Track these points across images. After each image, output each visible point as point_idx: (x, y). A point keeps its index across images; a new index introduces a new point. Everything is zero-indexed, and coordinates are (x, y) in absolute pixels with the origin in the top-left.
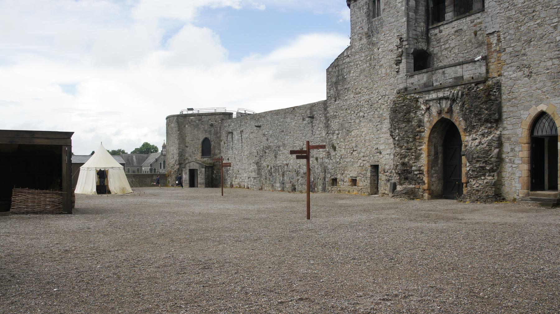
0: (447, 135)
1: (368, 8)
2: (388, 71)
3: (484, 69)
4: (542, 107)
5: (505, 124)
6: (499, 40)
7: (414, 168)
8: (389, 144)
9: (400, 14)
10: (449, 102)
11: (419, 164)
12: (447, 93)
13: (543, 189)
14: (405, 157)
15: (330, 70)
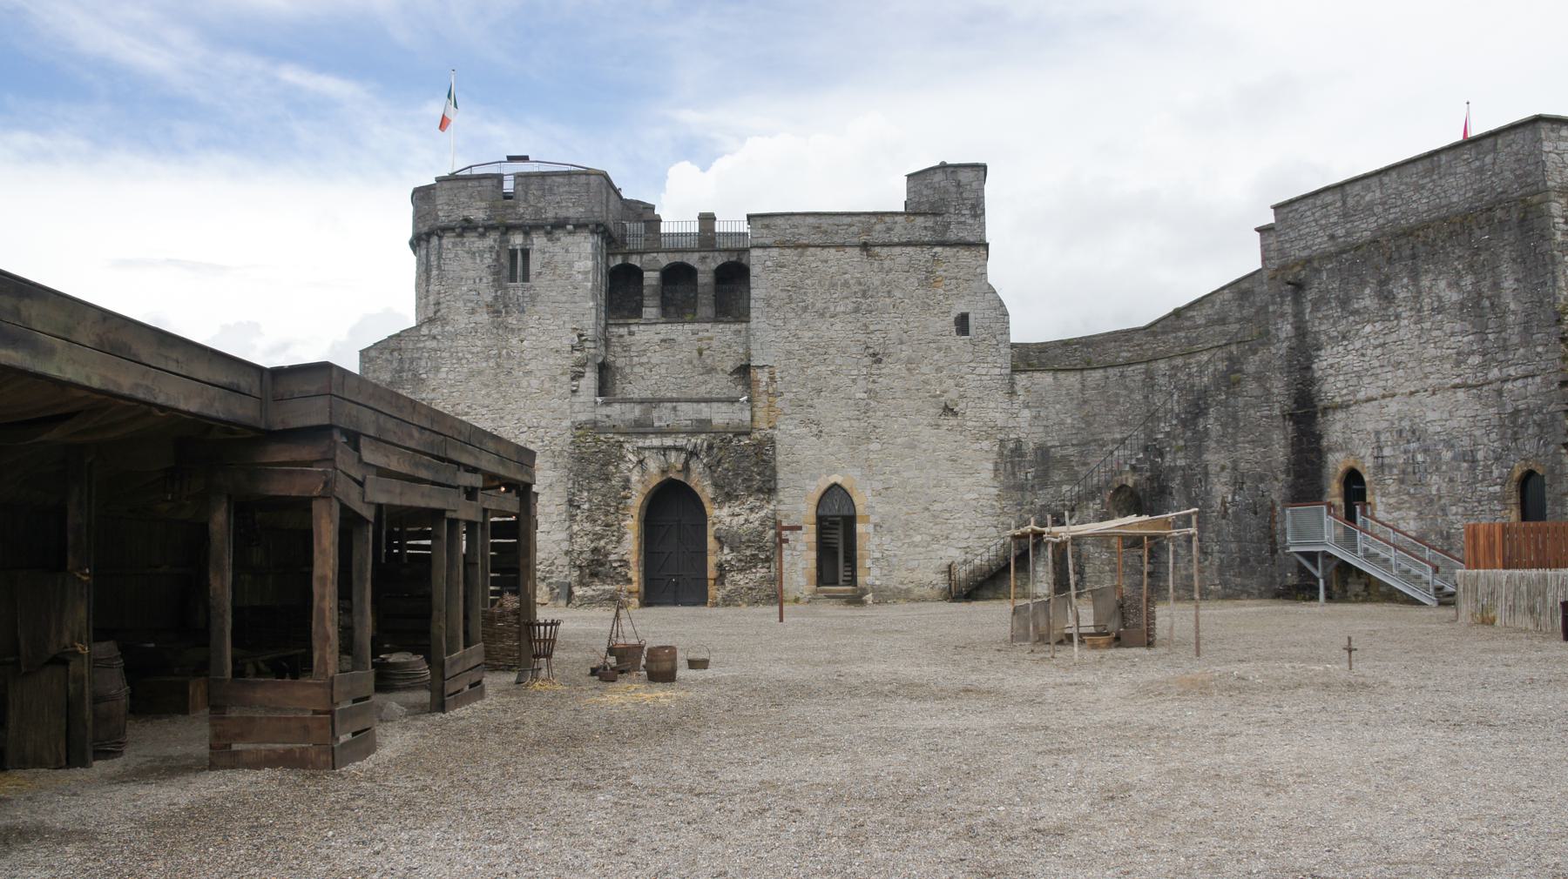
0: (671, 507)
1: (497, 260)
2: (547, 385)
3: (747, 416)
5: (781, 495)
6: (772, 379)
7: (612, 557)
9: (580, 292)
10: (683, 456)
11: (620, 550)
12: (681, 441)
13: (836, 583)
14: (602, 537)
15: (373, 353)
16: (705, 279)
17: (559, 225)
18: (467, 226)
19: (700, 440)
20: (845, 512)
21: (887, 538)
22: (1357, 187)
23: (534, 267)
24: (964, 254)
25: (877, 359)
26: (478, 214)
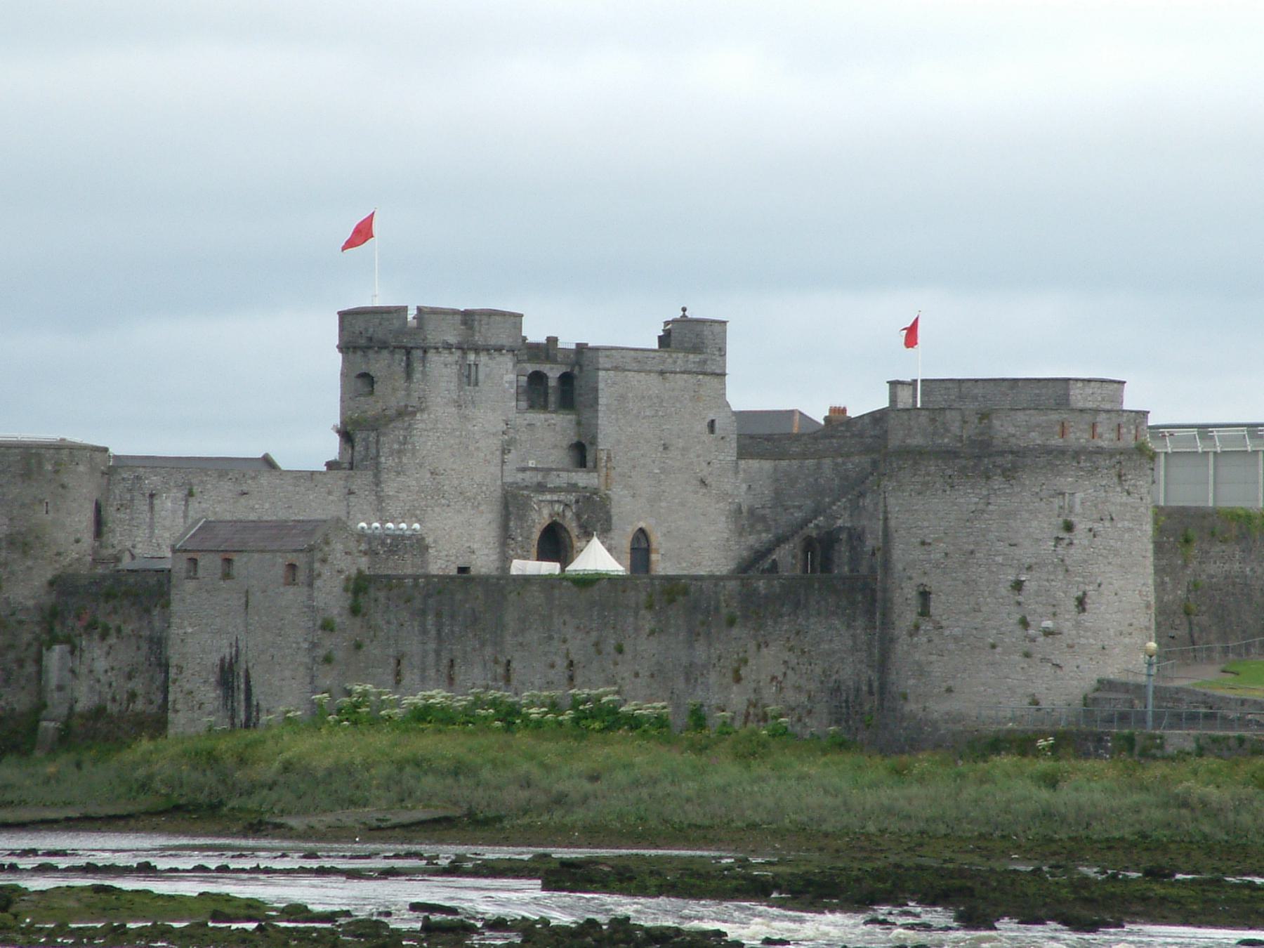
4: (642, 524)
5: (612, 534)
6: (609, 458)
8: (488, 543)
12: (562, 497)
16: (552, 383)
17: (499, 349)
18: (448, 347)
19: (572, 497)
20: (644, 545)
21: (668, 564)
22: (970, 384)
23: (481, 377)
24: (716, 380)
25: (666, 447)
26: (452, 340)
